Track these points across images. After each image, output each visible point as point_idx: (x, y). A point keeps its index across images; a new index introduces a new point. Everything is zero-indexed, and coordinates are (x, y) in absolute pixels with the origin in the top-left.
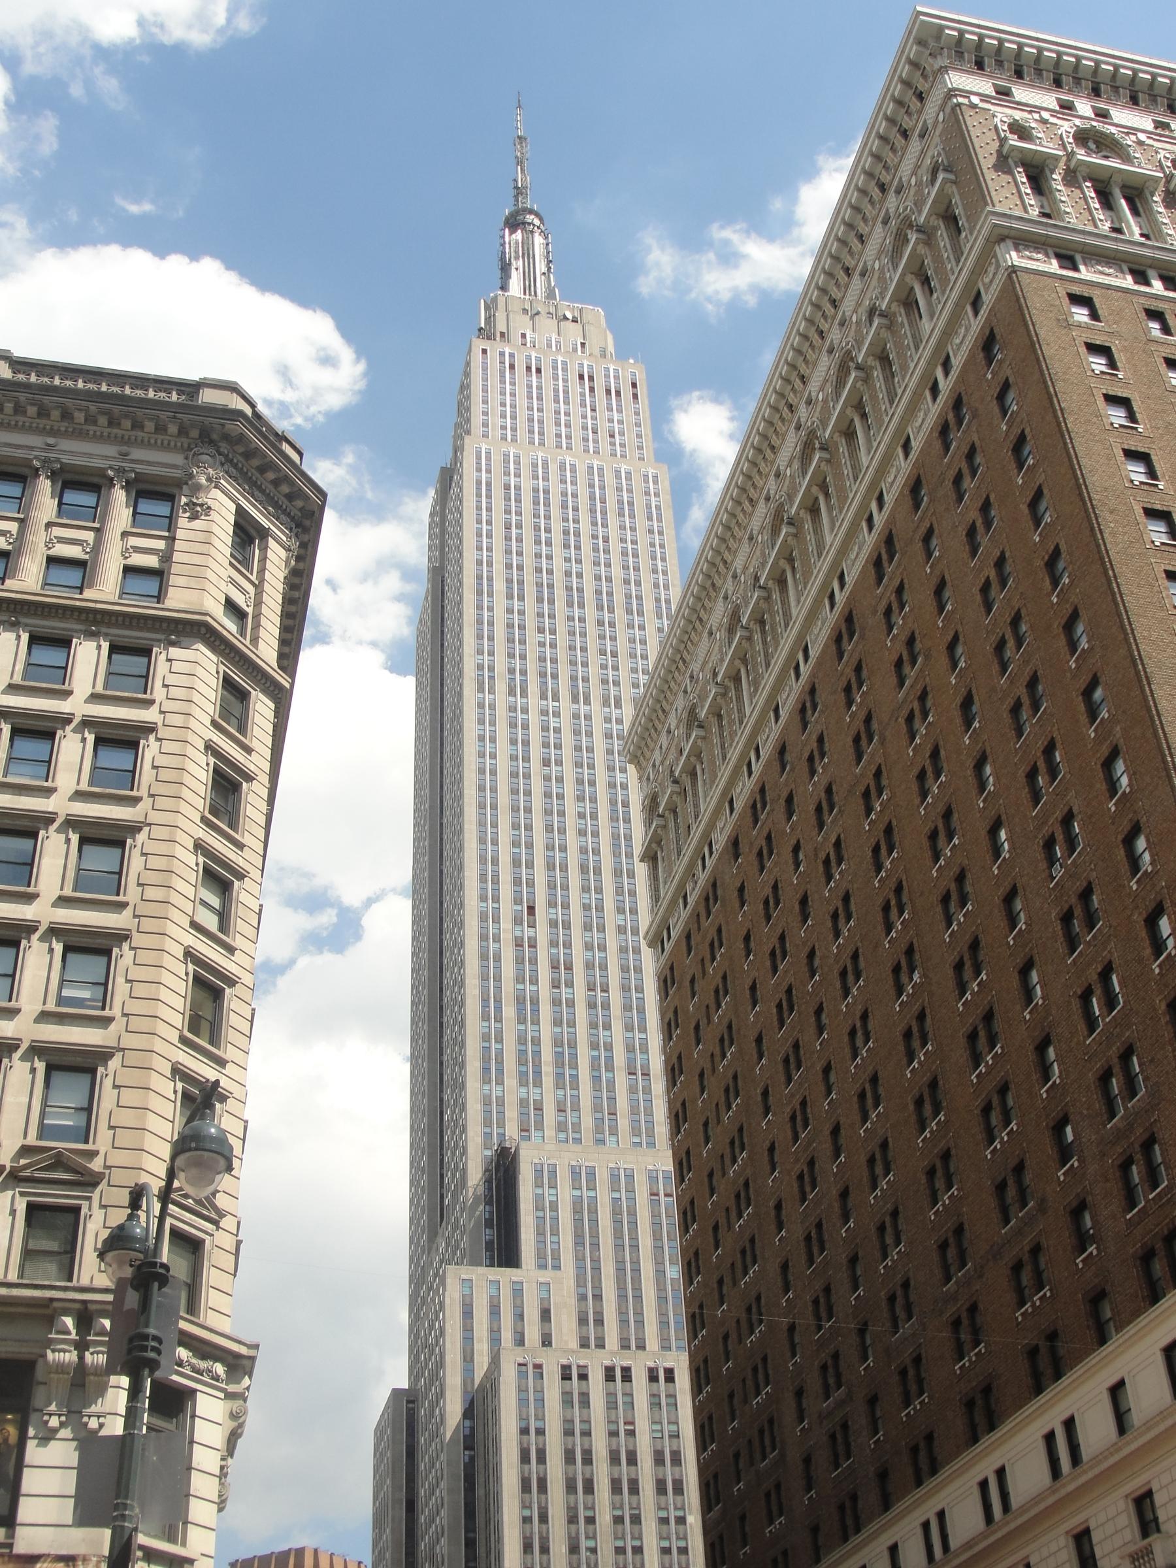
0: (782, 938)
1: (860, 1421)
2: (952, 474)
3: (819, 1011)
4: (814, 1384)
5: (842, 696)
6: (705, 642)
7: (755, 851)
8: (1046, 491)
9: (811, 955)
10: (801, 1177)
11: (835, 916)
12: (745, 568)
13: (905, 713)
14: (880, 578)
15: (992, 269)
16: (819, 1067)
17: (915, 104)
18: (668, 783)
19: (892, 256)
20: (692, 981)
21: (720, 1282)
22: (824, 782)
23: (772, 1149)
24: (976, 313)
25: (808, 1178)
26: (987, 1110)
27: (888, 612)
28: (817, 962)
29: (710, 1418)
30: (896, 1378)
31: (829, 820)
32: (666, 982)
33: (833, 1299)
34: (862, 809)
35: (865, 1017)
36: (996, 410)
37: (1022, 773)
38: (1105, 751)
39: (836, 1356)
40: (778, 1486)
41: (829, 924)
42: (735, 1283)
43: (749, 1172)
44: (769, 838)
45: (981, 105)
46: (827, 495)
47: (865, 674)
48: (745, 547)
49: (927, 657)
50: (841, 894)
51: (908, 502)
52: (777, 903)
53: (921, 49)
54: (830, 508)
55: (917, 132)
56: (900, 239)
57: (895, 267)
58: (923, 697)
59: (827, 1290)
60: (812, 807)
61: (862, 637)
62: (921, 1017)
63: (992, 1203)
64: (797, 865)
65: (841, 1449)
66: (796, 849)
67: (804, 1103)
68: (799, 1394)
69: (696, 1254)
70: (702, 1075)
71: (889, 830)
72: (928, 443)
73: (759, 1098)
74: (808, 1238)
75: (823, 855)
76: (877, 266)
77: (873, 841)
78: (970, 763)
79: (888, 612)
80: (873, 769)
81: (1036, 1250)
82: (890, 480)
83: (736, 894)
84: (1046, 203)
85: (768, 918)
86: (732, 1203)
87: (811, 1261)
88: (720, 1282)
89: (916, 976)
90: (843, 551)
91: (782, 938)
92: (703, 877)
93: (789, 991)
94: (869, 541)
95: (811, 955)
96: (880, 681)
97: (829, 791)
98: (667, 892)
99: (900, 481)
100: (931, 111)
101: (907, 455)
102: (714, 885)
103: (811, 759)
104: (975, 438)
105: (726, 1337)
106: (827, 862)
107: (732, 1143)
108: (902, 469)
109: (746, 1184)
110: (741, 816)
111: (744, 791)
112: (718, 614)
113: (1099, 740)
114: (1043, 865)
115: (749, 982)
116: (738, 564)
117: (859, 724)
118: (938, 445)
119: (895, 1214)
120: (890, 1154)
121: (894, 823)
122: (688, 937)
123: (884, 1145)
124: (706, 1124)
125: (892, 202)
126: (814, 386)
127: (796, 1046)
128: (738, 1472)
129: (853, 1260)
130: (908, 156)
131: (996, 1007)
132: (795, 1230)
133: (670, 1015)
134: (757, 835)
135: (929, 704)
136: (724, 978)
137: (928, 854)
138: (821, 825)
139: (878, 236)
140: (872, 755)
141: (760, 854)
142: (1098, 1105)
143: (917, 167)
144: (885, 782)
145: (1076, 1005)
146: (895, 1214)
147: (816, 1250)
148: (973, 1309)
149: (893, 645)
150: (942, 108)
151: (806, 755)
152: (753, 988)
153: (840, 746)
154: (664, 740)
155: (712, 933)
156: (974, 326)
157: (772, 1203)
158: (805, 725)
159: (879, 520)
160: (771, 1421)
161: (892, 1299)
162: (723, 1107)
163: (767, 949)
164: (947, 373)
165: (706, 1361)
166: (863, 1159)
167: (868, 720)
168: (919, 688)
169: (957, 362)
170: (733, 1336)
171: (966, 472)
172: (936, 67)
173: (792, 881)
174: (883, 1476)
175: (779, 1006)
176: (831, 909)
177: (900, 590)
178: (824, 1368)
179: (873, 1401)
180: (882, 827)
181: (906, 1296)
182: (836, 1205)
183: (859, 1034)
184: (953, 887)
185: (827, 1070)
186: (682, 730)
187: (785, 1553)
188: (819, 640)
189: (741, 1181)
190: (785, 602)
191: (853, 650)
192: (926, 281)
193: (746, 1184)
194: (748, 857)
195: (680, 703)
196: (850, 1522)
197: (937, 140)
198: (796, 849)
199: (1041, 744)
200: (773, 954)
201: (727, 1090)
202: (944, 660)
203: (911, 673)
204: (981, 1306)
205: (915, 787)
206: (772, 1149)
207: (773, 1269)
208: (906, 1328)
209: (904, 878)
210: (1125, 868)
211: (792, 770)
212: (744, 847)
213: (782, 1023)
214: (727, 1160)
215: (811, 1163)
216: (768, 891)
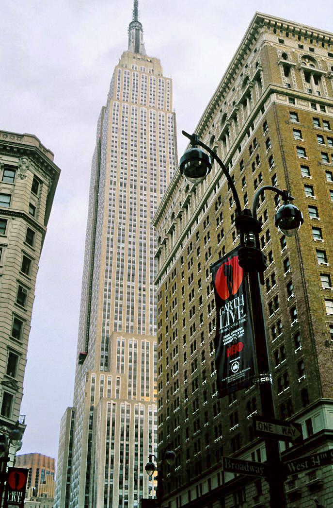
0: (193, 291)
7: (187, 263)
9: (201, 298)
31: (209, 258)
41: (206, 290)
43: (178, 360)
45: (274, 46)
52: (192, 280)
53: (257, 25)
55: (254, 51)
56: (245, 83)
57: (243, 92)
60: (205, 253)
61: (222, 205)
64: (199, 269)
66: (199, 265)
73: (183, 338)
75: (206, 269)
76: (237, 90)
82: (234, 159)
85: (190, 284)
91: (193, 291)
93: (194, 307)
97: (210, 249)
100: (258, 46)
109: (177, 363)
110: (184, 251)
117: (219, 231)
124: (167, 343)
125: (244, 70)
126: (215, 122)
127: (194, 325)
130: (250, 57)
136: (176, 299)
138: (207, 259)
141: (189, 264)
143: (252, 62)
150: (262, 45)
151: (204, 237)
153: (214, 236)
157: (184, 371)
158: (205, 227)
162: (172, 339)
163: (188, 293)
167: (222, 231)
172: (261, 32)
173: (197, 274)
175: (191, 311)
176: (207, 285)
190: (202, 187)
191: (220, 208)
198: (199, 265)
207: (183, 390)
211: (200, 240)
213: (191, 317)
216: (190, 276)
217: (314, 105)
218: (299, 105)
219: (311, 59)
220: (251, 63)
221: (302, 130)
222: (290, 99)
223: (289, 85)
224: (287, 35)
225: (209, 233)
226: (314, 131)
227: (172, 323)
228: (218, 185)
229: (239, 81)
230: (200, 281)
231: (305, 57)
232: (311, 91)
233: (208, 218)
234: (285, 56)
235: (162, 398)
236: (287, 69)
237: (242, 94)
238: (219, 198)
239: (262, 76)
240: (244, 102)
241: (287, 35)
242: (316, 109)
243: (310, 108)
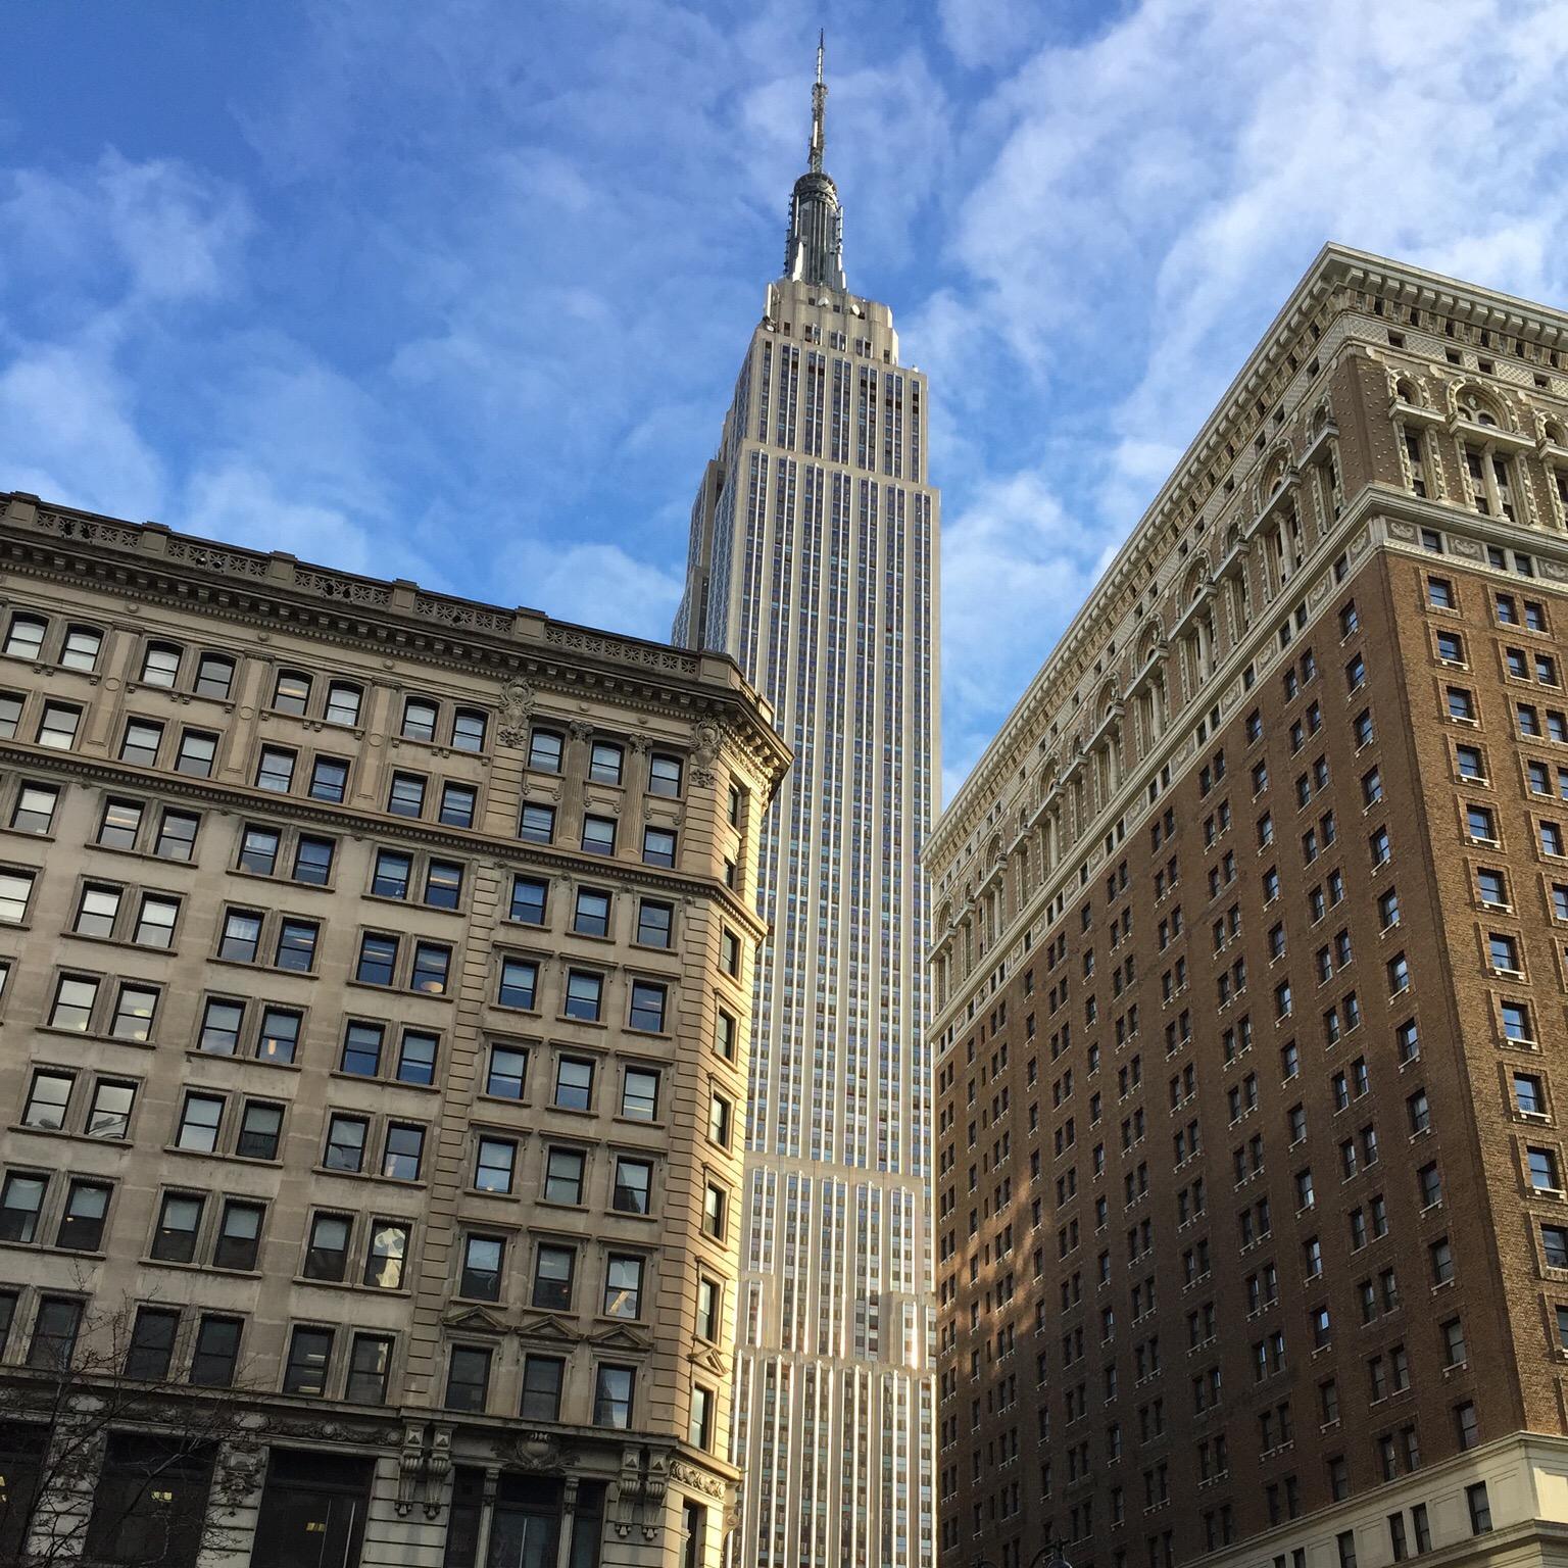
13: (1214, 919)
17: (1309, 337)
19: (1261, 484)
27: (1209, 823)
51: (1243, 730)
79: (1209, 823)
84: (1421, 471)
99: (1237, 707)
121: (1191, 1012)
140: (1176, 946)
149: (1209, 856)
172: (1339, 307)
177: (1223, 807)
192: (1292, 520)
197: (1325, 384)
205: (1215, 987)
209: (1195, 1063)
224: (1414, 319)
232: (1483, 504)
240: (1269, 531)
241: (1414, 319)
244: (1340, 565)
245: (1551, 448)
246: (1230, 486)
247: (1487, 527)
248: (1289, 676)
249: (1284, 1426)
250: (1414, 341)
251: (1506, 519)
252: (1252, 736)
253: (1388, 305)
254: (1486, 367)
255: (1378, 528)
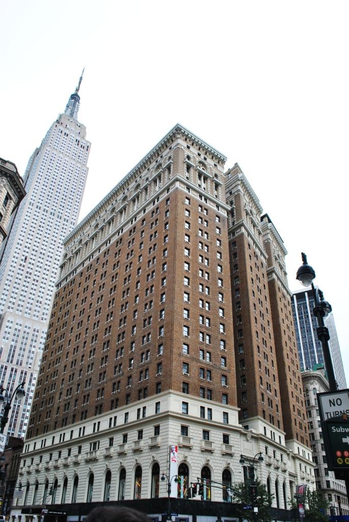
0: (86, 298)
1: (72, 403)
2: (151, 222)
3: (89, 316)
4: (65, 392)
5: (114, 255)
6: (89, 227)
8: (168, 236)
9: (91, 304)
10: (75, 349)
11: (99, 299)
12: (102, 217)
13: (126, 265)
14: (130, 235)
15: (173, 186)
16: (85, 328)
17: (171, 141)
18: (71, 253)
20: (63, 298)
21: (50, 364)
22: (105, 270)
23: (70, 341)
24: (167, 193)
25: (76, 349)
26: (118, 351)
27: (129, 243)
28: (92, 306)
29: (39, 392)
30: (83, 397)
31: (103, 278)
32: (57, 295)
33: (74, 377)
34: (111, 280)
35: (98, 322)
36: (164, 214)
37: (145, 288)
38: (162, 292)
39: (71, 389)
40: (50, 411)
42: (53, 366)
44: (89, 276)
46: (125, 211)
47: (120, 253)
48: (104, 212)
49: (134, 256)
50: (101, 295)
51: (141, 222)
54: (125, 214)
58: (131, 263)
59: (73, 374)
60: (101, 274)
61: (122, 245)
62: (110, 327)
63: (113, 370)
64: (94, 284)
65: (67, 408)
66: (95, 281)
67: (80, 334)
68: (61, 394)
69: (46, 356)
70: (59, 319)
71: (115, 287)
72: (149, 213)
74: (72, 362)
77: (111, 287)
78: (136, 281)
79: (129, 243)
80: (116, 273)
81: (119, 382)
83: (78, 284)
85: (84, 292)
86: (58, 349)
87: (72, 367)
88: (50, 364)
89: (112, 318)
90: (125, 225)
91: (86, 298)
92: (72, 277)
93: (84, 309)
94: (130, 226)
95: (91, 304)
96: (123, 256)
97: (105, 272)
98: (63, 276)
100: (173, 145)
101: (144, 213)
102: (74, 280)
103: (104, 264)
104: (159, 218)
105: (48, 376)
106: (100, 287)
107: (61, 336)
108: (142, 215)
111: (87, 263)
112: (93, 223)
113: (162, 290)
114: (144, 308)
115: (75, 304)
116: (102, 215)
117: (116, 262)
118: (151, 215)
119: (93, 364)
120: (95, 352)
122: (65, 288)
123: (95, 349)
124: (57, 330)
125: (159, 159)
126: (130, 187)
128: (42, 406)
129: (81, 370)
131: (126, 332)
132: (70, 359)
133: (55, 303)
134: (87, 274)
135: (132, 265)
136: (70, 300)
137: (122, 295)
139: (154, 164)
141: (86, 278)
142: (140, 359)
144: (117, 276)
145: (141, 338)
146: (93, 364)
147: (73, 365)
148: (103, 389)
150: (176, 146)
152: (76, 305)
153: (110, 265)
154: (73, 243)
155: (71, 290)
156: (165, 195)
158: (105, 256)
159: (134, 222)
160: (53, 397)
161: (87, 381)
163: (82, 299)
164: (157, 201)
165: (41, 380)
166: (89, 350)
167: (118, 262)
168: (131, 261)
169: (160, 200)
170: (49, 377)
171: (154, 223)
174: (74, 416)
175: (81, 312)
177: (133, 239)
178: (68, 390)
179: (76, 400)
180: (114, 285)
181: (90, 381)
182: (81, 358)
183: (96, 325)
184: (125, 304)
185: (87, 329)
186: (77, 243)
187: (48, 426)
188: (113, 240)
189: (61, 345)
190: (109, 228)
192: (160, 179)
193: (62, 346)
194: (83, 278)
195: (79, 237)
196: (64, 423)
198: (95, 281)
199: (151, 285)
200: (83, 300)
201: (64, 324)
202: (138, 259)
203: (130, 258)
204: (105, 389)
205: (124, 280)
206: (70, 341)
208: (88, 388)
210: (159, 316)
212: (83, 275)
214: (59, 339)
215: (78, 347)
216: (86, 287)
217: (201, 197)
218: (192, 194)
219: (204, 164)
220: (166, 155)
221: (191, 211)
222: (187, 188)
223: (187, 178)
224: (193, 144)
225: (107, 261)
226: (198, 213)
227: (64, 317)
228: (122, 230)
229: (154, 164)
230: (93, 292)
231: (200, 162)
232: (200, 186)
233: (109, 250)
234: (188, 157)
235: (44, 368)
236: (189, 167)
237: (155, 175)
238: (121, 240)
239: (172, 167)
240: (155, 181)
241: (193, 144)
242: (201, 199)
243: (198, 198)
244: (168, 190)
245: (215, 179)
246: (148, 170)
247: (200, 190)
248: (153, 212)
249: (118, 386)
250: (192, 148)
251: (203, 190)
252: (142, 224)
253: (188, 140)
254: (205, 159)
255: (178, 184)
